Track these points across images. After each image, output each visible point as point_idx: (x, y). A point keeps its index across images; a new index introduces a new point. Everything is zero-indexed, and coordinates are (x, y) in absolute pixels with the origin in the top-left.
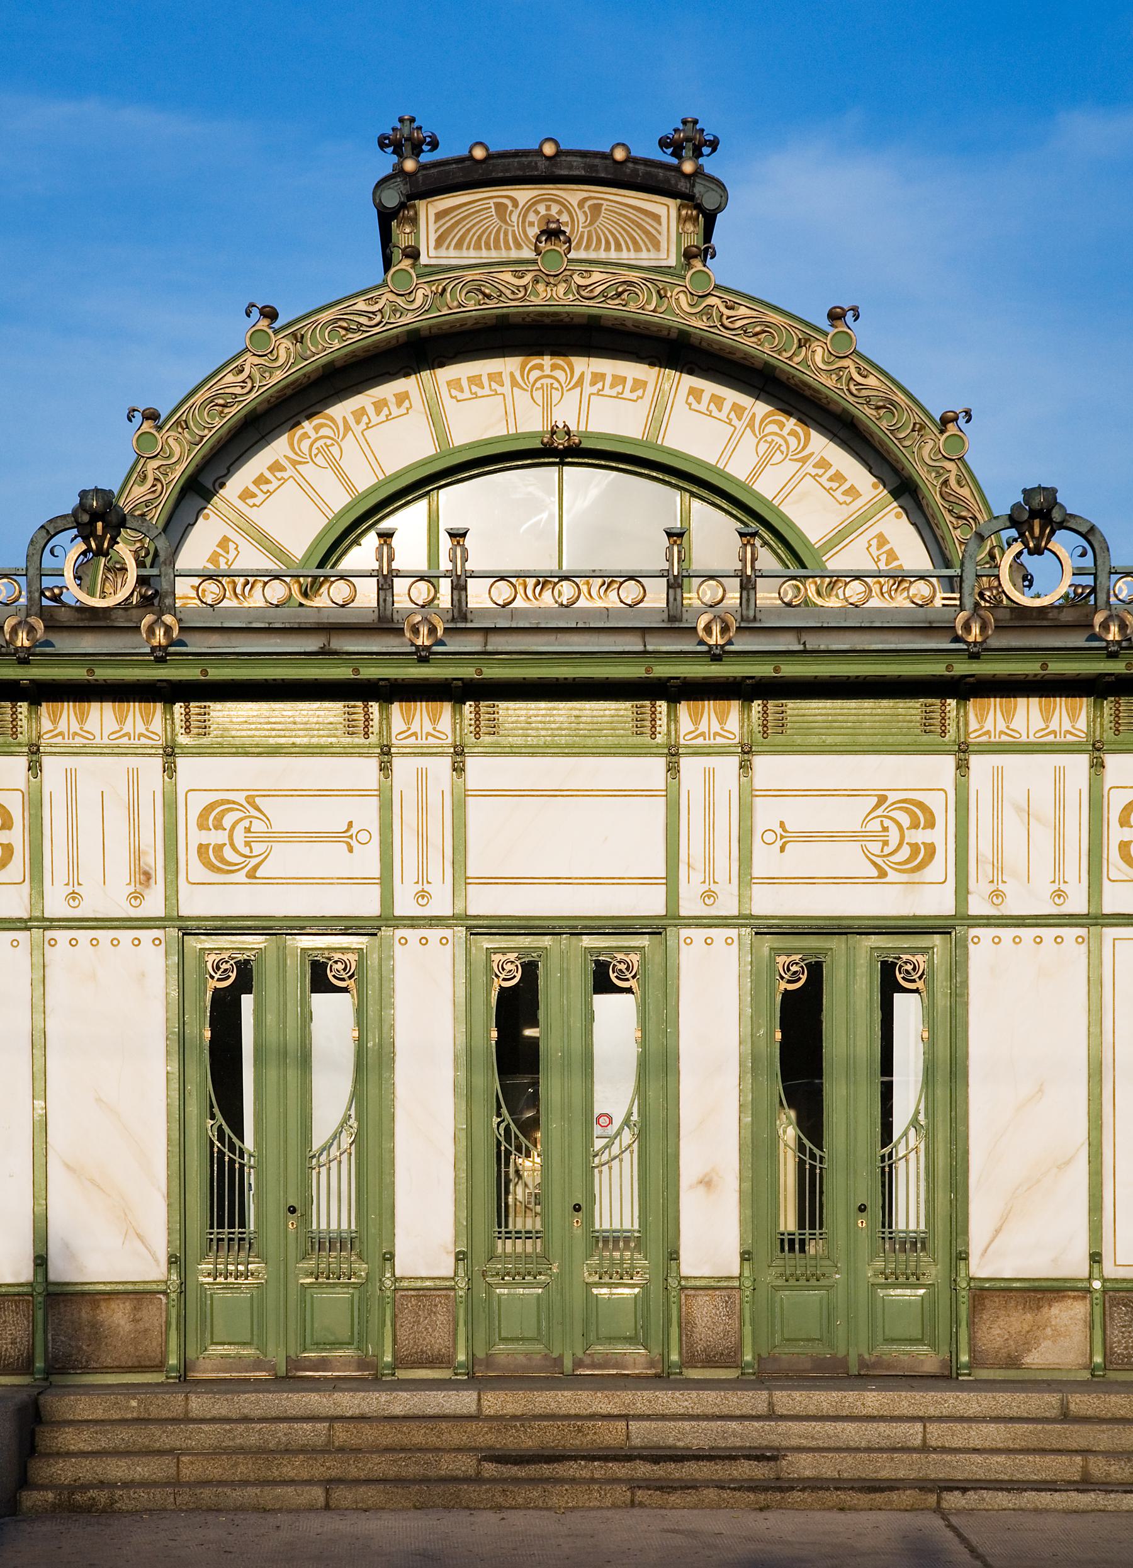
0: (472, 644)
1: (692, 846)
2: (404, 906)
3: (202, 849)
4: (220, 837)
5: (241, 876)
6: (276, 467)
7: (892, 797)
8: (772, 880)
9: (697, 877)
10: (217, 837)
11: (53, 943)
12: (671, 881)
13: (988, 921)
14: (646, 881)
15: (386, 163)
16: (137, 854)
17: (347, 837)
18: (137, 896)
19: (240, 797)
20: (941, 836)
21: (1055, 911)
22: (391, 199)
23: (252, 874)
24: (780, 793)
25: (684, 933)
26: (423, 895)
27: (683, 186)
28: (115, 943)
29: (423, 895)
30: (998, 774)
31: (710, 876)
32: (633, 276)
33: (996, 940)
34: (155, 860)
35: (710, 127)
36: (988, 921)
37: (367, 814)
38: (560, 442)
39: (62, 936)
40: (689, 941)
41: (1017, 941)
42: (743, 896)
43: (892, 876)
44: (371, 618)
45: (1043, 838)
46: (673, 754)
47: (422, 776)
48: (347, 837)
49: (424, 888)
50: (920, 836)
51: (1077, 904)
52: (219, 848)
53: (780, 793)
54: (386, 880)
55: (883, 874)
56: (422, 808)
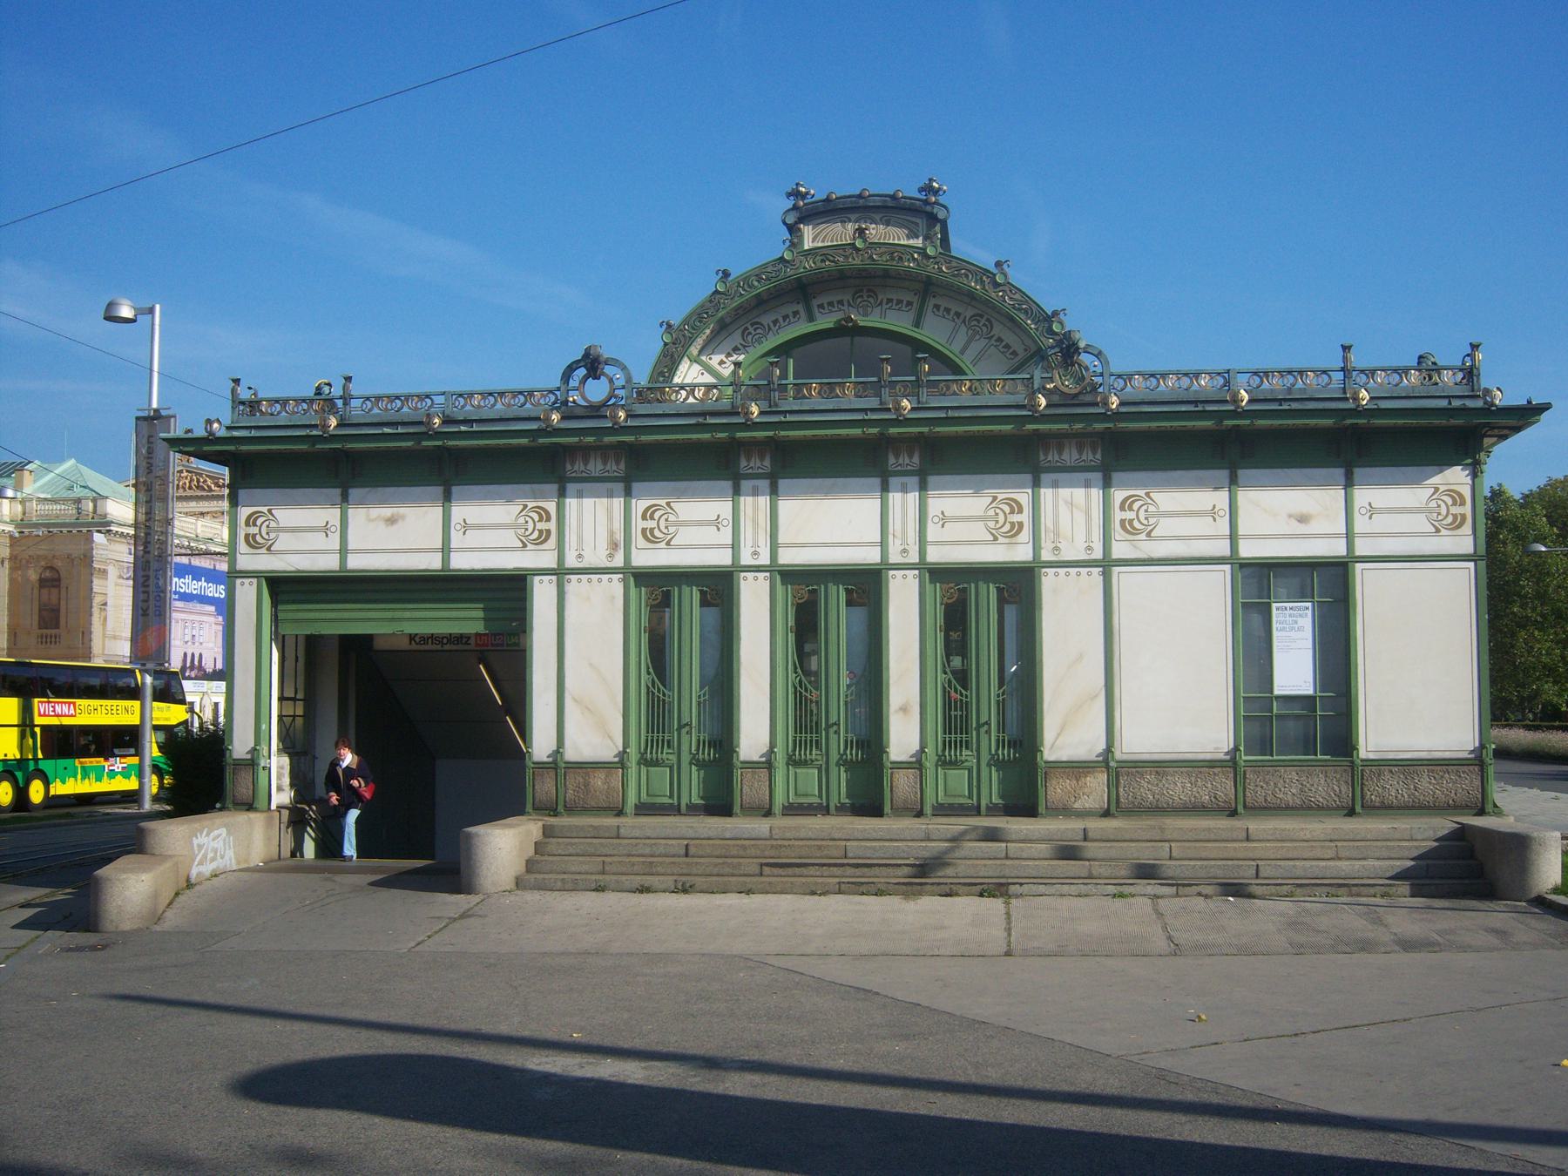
4: (652, 524)
5: (663, 545)
8: (937, 543)
9: (898, 542)
10: (651, 524)
11: (569, 581)
12: (883, 544)
13: (1051, 564)
14: (871, 544)
15: (790, 204)
16: (611, 533)
17: (717, 523)
18: (611, 556)
21: (1086, 557)
22: (791, 220)
23: (668, 543)
25: (891, 573)
26: (755, 553)
27: (928, 208)
28: (600, 581)
29: (755, 553)
31: (904, 541)
33: (1056, 574)
34: (620, 537)
36: (1051, 564)
40: (894, 577)
41: (1067, 574)
42: (922, 553)
43: (1001, 540)
44: (728, 408)
45: (1080, 518)
49: (755, 550)
50: (1016, 518)
51: (1098, 554)
52: (652, 530)
54: (735, 547)
55: (996, 539)
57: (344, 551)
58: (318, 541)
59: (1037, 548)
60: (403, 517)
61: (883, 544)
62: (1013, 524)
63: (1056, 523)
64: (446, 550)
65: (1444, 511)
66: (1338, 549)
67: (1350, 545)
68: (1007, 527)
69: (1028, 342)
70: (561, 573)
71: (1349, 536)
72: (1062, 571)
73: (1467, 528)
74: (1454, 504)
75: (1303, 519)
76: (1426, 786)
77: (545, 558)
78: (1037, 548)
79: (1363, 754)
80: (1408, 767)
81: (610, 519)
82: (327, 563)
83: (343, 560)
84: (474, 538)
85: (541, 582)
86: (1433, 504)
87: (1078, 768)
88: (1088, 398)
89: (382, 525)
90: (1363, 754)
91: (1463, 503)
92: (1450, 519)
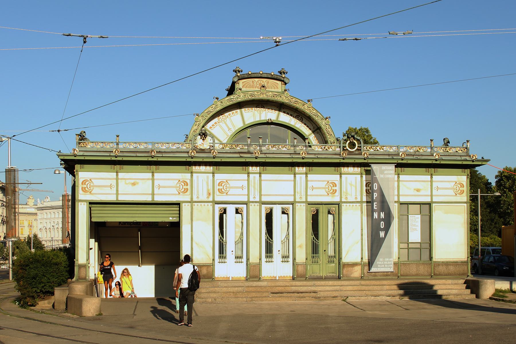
0: (263, 156)
1: (298, 189)
2: (251, 199)
3: (219, 189)
4: (222, 187)
5: (225, 194)
6: (216, 123)
7: (330, 182)
10: (221, 187)
11: (194, 205)
12: (294, 195)
13: (345, 202)
16: (208, 190)
17: (242, 188)
18: (208, 197)
19: (225, 181)
20: (337, 188)
23: (227, 194)
24: (312, 181)
27: (282, 79)
30: (346, 178)
31: (301, 195)
32: (276, 93)
35: (286, 70)
36: (345, 202)
37: (245, 183)
38: (270, 121)
39: (196, 204)
42: (306, 198)
43: (330, 195)
46: (295, 174)
47: (254, 177)
48: (242, 188)
50: (334, 188)
53: (312, 181)
56: (254, 183)
57: (117, 194)
58: (108, 190)
59: (341, 198)
60: (138, 183)
61: (294, 195)
62: (333, 190)
63: (346, 190)
64: (153, 194)
65: (458, 189)
66: (428, 200)
67: (432, 199)
68: (332, 191)
69: (314, 125)
70: (192, 202)
71: (432, 196)
72: (348, 204)
73: (465, 194)
74: (461, 187)
75: (418, 190)
76: (452, 268)
77: (186, 197)
78: (341, 198)
79: (434, 260)
80: (447, 264)
81: (208, 185)
82: (112, 198)
83: (117, 197)
84: (162, 191)
85: (185, 205)
86: (455, 187)
87: (354, 265)
88: (357, 152)
89: (131, 185)
90: (434, 260)
91: (463, 187)
92: (460, 191)
